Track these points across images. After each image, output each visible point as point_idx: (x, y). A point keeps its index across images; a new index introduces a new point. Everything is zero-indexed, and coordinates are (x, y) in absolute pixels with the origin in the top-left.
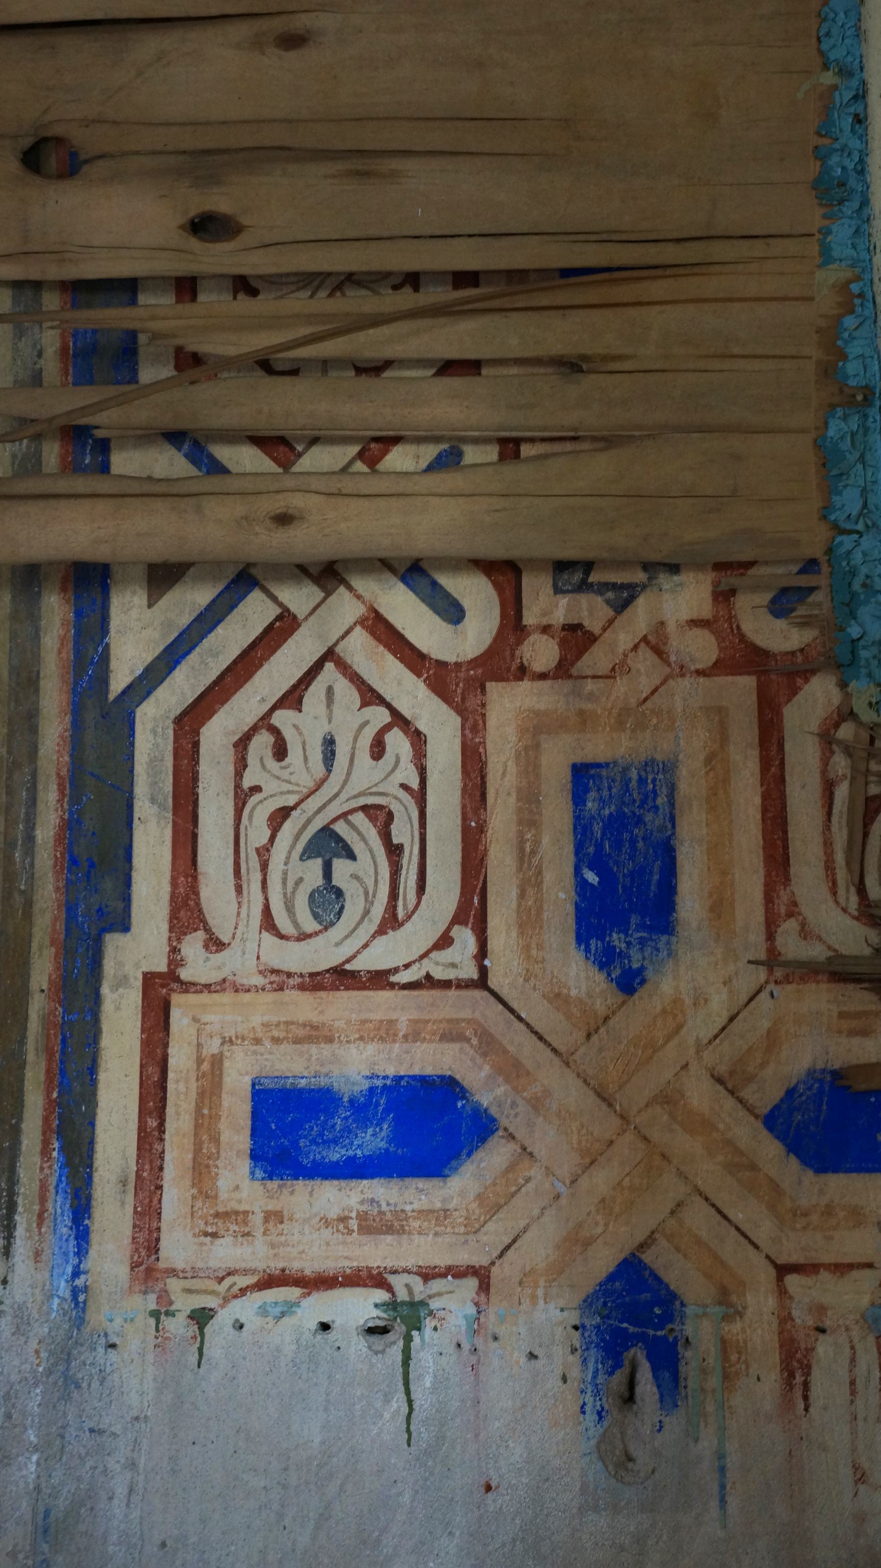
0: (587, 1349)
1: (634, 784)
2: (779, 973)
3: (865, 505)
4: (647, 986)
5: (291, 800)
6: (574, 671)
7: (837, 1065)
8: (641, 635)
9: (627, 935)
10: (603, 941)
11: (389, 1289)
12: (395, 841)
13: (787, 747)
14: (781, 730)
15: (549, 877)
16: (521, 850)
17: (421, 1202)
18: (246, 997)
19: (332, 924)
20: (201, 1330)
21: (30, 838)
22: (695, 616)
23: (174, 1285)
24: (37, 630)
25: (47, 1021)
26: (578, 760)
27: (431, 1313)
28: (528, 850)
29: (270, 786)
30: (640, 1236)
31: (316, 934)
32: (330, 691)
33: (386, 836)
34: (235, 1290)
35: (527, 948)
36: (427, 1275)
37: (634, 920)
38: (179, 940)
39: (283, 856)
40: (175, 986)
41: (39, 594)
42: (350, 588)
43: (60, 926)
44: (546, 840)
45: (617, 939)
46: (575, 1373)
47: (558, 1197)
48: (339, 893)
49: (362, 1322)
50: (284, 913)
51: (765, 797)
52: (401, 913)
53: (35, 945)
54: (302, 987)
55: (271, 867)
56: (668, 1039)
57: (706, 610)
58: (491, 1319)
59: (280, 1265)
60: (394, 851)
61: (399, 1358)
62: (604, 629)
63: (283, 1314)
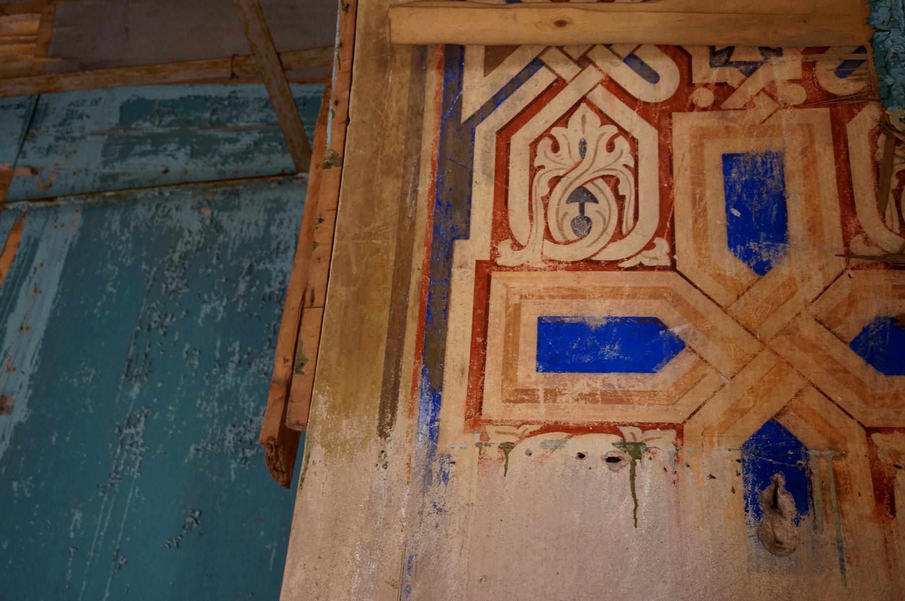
0: (747, 473)
1: (759, 164)
2: (854, 262)
3: (892, 16)
4: (772, 271)
5: (561, 173)
6: (723, 106)
7: (894, 315)
8: (761, 88)
9: (759, 243)
10: (744, 246)
11: (621, 435)
12: (621, 194)
13: (850, 144)
14: (845, 136)
15: (710, 213)
16: (694, 199)
17: (640, 387)
18: (535, 274)
19: (585, 236)
20: (506, 454)
21: (415, 191)
22: (792, 77)
23: (490, 429)
24: (424, 88)
25: (422, 285)
26: (726, 152)
27: (647, 450)
28: (698, 196)
29: (549, 166)
30: (777, 409)
31: (576, 241)
32: (584, 118)
33: (615, 190)
34: (527, 433)
35: (699, 250)
36: (644, 427)
37: (763, 235)
38: (497, 244)
39: (556, 201)
40: (494, 268)
41: (426, 70)
42: (595, 66)
43: (430, 236)
44: (708, 193)
45: (753, 245)
46: (740, 487)
47: (723, 385)
48: (588, 220)
49: (604, 453)
50: (557, 230)
51: (838, 171)
52: (624, 231)
53: (415, 245)
54: (567, 269)
55: (549, 207)
56: (787, 299)
57: (799, 74)
58: (686, 453)
59: (554, 420)
60: (620, 199)
61: (628, 475)
62: (740, 85)
63: (556, 447)
